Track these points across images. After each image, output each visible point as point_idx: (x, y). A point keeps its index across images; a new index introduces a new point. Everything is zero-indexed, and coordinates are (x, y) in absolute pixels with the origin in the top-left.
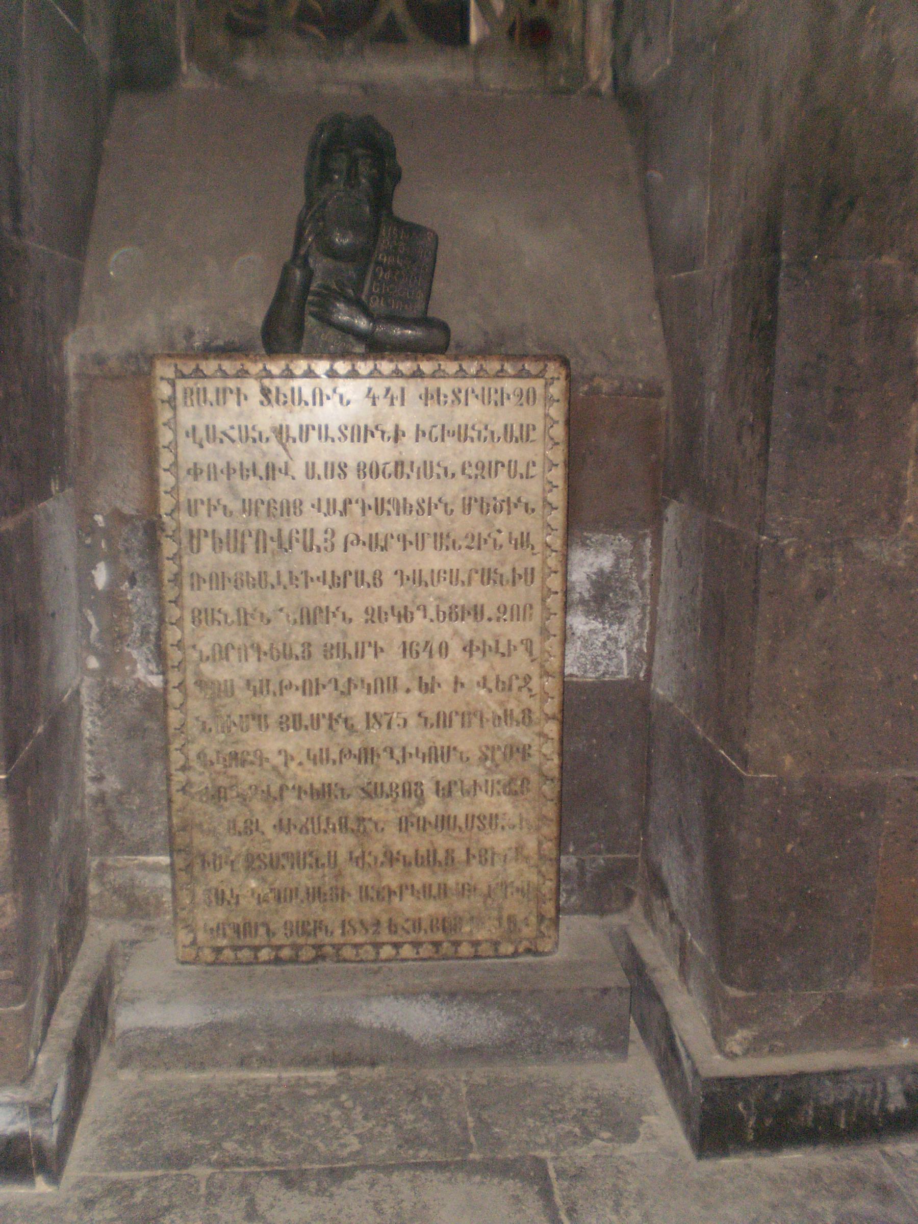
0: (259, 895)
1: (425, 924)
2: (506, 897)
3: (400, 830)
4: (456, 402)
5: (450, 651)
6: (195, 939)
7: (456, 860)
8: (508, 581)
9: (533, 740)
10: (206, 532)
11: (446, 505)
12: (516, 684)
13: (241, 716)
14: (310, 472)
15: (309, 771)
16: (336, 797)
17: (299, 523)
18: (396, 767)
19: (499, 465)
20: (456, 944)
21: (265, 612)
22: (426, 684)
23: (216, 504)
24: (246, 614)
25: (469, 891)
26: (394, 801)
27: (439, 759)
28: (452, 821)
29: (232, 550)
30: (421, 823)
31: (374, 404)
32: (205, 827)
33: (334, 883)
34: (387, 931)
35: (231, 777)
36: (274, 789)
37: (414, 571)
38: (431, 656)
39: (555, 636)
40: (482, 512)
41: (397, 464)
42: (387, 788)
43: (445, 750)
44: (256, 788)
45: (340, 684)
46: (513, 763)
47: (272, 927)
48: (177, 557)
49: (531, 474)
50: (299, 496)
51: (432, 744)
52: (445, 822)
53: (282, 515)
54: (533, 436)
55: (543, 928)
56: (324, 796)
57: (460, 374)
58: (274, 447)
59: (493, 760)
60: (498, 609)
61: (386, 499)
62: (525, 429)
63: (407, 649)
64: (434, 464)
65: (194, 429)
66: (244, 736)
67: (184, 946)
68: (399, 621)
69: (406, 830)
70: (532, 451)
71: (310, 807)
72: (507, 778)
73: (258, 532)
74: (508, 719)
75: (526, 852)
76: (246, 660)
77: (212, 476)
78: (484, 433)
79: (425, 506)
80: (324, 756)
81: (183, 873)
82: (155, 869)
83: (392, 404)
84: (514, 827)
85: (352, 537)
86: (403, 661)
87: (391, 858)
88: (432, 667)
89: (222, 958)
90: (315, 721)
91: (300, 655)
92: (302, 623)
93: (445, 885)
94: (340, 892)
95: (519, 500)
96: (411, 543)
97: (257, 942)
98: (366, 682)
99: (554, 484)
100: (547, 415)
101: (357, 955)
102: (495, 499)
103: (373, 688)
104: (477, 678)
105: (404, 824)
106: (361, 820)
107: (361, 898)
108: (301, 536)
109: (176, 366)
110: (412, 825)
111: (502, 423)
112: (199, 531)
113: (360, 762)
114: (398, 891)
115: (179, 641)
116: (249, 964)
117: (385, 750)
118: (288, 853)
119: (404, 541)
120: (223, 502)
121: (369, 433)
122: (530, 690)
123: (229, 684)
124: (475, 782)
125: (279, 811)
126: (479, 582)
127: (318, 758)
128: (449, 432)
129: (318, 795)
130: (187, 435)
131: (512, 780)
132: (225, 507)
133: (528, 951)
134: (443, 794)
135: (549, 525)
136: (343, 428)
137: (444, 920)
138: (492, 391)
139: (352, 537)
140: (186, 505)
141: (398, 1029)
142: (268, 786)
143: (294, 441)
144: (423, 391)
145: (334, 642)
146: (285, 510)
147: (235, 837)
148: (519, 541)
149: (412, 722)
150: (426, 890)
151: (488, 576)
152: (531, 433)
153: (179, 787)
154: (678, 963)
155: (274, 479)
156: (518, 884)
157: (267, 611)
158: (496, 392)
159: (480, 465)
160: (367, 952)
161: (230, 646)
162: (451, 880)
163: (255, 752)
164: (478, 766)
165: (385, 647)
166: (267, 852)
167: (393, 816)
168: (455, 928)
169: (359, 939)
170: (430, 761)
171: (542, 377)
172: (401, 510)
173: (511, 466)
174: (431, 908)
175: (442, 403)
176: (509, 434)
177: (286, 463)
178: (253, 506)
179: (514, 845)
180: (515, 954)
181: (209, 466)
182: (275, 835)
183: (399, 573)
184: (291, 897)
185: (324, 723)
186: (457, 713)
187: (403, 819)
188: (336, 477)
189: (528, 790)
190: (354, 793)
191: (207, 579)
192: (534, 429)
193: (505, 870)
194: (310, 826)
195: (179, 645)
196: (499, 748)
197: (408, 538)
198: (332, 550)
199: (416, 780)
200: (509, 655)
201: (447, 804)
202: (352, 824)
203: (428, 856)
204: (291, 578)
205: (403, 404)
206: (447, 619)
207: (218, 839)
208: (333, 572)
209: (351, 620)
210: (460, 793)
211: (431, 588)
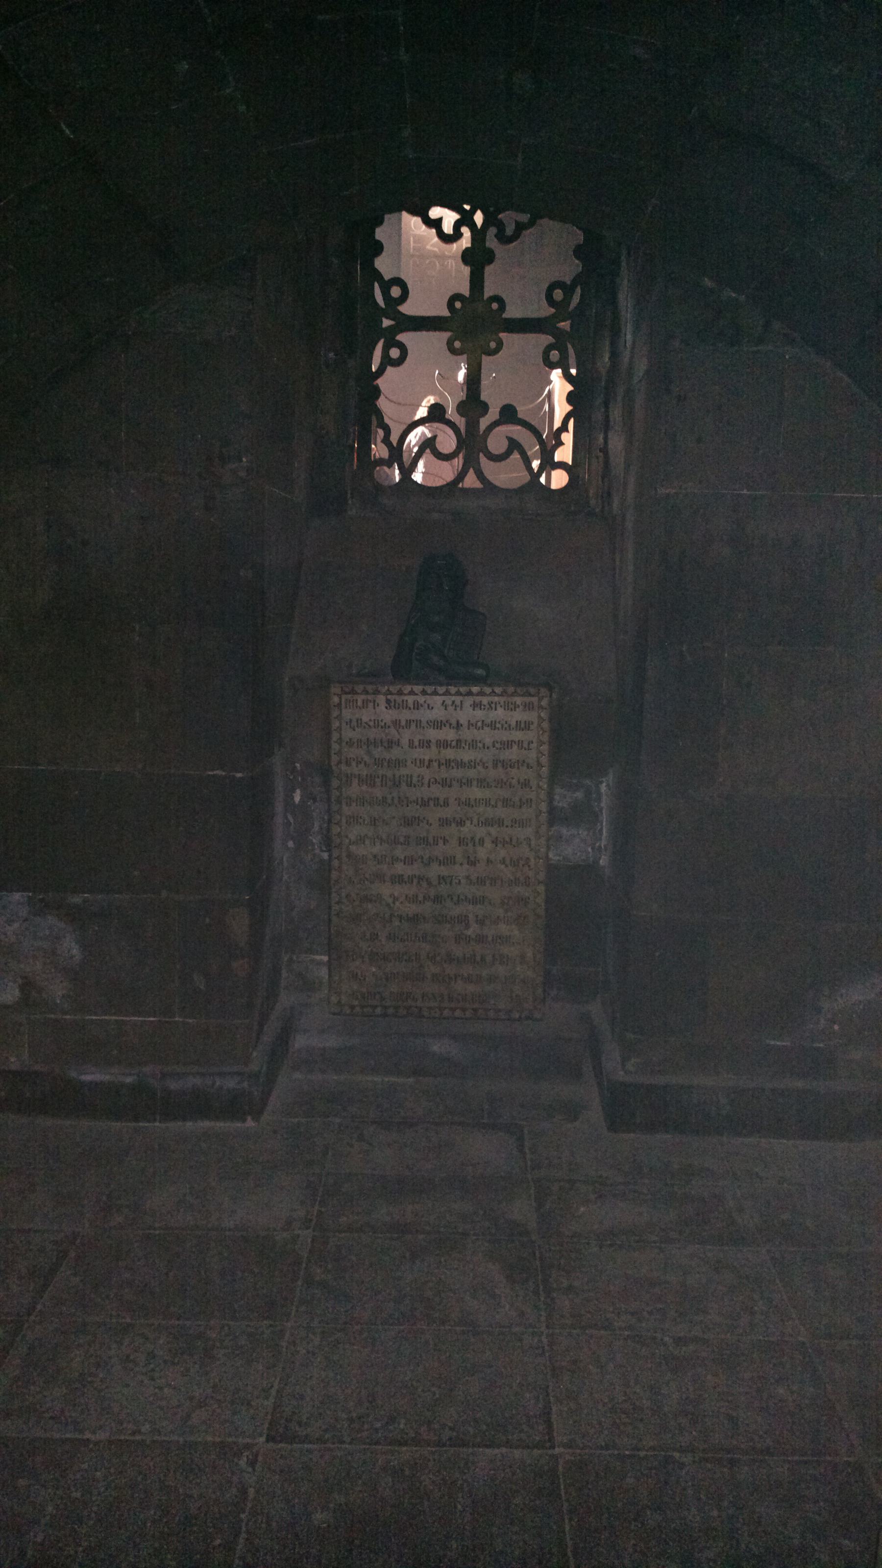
12: (522, 863)
17: (404, 771)
31: (446, 709)
38: (474, 845)
41: (457, 740)
45: (425, 861)
48: (339, 788)
52: (481, 939)
54: (532, 727)
58: (393, 731)
63: (461, 841)
64: (478, 741)
79: (473, 764)
82: (319, 963)
83: (456, 710)
86: (459, 848)
87: (450, 958)
88: (475, 852)
89: (354, 1011)
90: (411, 879)
102: (510, 760)
108: (405, 778)
109: (342, 688)
114: (454, 977)
117: (448, 896)
122: (529, 866)
132: (365, 762)
144: (472, 703)
151: (506, 802)
152: (531, 726)
169: (433, 1004)
173: (520, 743)
174: (471, 988)
185: (415, 881)
208: (422, 799)
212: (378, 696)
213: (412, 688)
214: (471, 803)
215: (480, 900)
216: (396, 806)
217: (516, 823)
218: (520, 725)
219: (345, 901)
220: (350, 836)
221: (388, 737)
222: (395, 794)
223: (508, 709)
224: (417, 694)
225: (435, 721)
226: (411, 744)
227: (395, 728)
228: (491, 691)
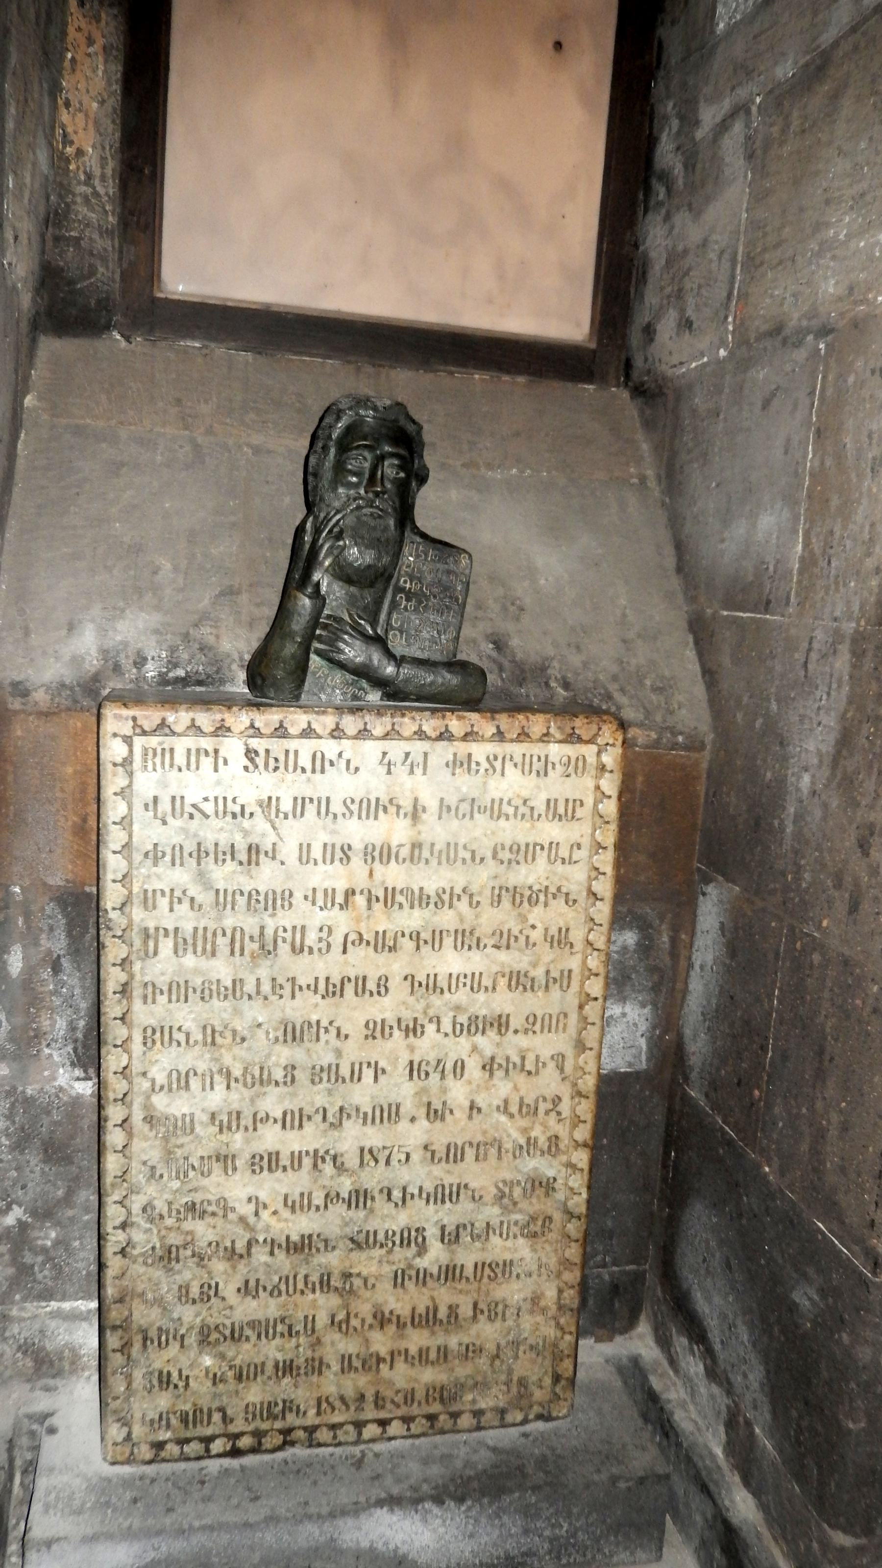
0: (215, 1375)
1: (420, 1395)
2: (516, 1357)
3: (395, 1285)
4: (491, 771)
5: (466, 1070)
6: (129, 1434)
7: (460, 1317)
8: (540, 988)
9: (559, 1171)
10: (166, 930)
11: (471, 896)
13: (202, 1158)
14: (305, 854)
15: (286, 1220)
16: (318, 1250)
17: (286, 919)
18: (394, 1211)
19: (538, 848)
20: (455, 1416)
21: (239, 1028)
22: (436, 1111)
23: (181, 895)
25: (474, 1352)
26: (390, 1252)
27: (447, 1199)
28: (458, 1271)
29: (199, 954)
30: (421, 1275)
31: (389, 772)
32: (150, 1296)
33: (309, 1353)
34: (372, 1406)
35: (187, 1233)
36: (240, 1246)
38: (443, 1077)
39: (591, 1049)
40: (514, 904)
42: (381, 1237)
43: (455, 1189)
44: (218, 1244)
46: (534, 1200)
47: (229, 1412)
49: (575, 858)
50: (289, 885)
51: (439, 1182)
53: (266, 909)
54: (579, 813)
55: (558, 1390)
58: (260, 825)
59: (511, 1195)
60: (527, 1019)
61: (399, 888)
64: (460, 848)
65: (156, 799)
66: (205, 1182)
67: (115, 1444)
68: (407, 1036)
70: (580, 831)
71: (283, 1261)
72: (527, 1218)
73: (235, 929)
75: (543, 1303)
76: (212, 1088)
77: (178, 861)
79: (446, 897)
81: (119, 1354)
82: (75, 1317)
83: (412, 772)
85: (353, 937)
87: (382, 1320)
88: (444, 1090)
89: (163, 1454)
90: (297, 1160)
91: (280, 1079)
92: (285, 1041)
93: (446, 1347)
94: (317, 1364)
95: (559, 889)
96: (426, 942)
97: (209, 1431)
98: (362, 1111)
99: (601, 870)
100: (598, 788)
101: (335, 1437)
102: (530, 888)
104: (496, 1102)
105: (399, 1280)
106: (347, 1276)
107: (343, 1371)
108: (288, 935)
109: (134, 719)
110: (410, 1278)
111: (543, 797)
112: (157, 929)
113: (349, 1206)
114: (388, 1359)
115: (125, 1068)
116: (199, 1458)
117: (381, 1191)
118: (254, 1321)
119: (418, 938)
120: (190, 893)
121: (381, 808)
122: (559, 1113)
123: (188, 1119)
124: (488, 1224)
125: (245, 1271)
126: (505, 987)
127: (298, 1205)
129: (295, 1249)
130: (146, 806)
131: (533, 1219)
132: (192, 899)
133: (540, 1417)
134: (450, 1240)
135: (592, 920)
136: (349, 801)
137: (442, 1388)
138: (535, 759)
139: (353, 937)
140: (142, 896)
141: (391, 1546)
142: (233, 1242)
143: (286, 817)
144: (451, 758)
145: (325, 1063)
146: (270, 902)
147: (187, 1306)
148: (556, 938)
149: (415, 1157)
150: (423, 1356)
153: (117, 1249)
154: (723, 1436)
155: (257, 864)
156: (532, 1341)
157: (240, 1026)
159: (515, 847)
160: (346, 1433)
162: (453, 1342)
163: (218, 1201)
164: (493, 1204)
165: (388, 1069)
166: (228, 1323)
167: (388, 1270)
168: (454, 1398)
169: (337, 1418)
170: (435, 1202)
171: (593, 743)
172: (416, 902)
174: (428, 1375)
175: (473, 772)
176: (552, 810)
177: (274, 844)
178: (229, 898)
179: (529, 1296)
180: (525, 1421)
181: (174, 848)
182: (240, 1299)
183: (409, 978)
184: (256, 1375)
186: (471, 1144)
187: (400, 1272)
189: (550, 1230)
190: (341, 1245)
191: (165, 988)
192: (582, 805)
193: (518, 1326)
194: (283, 1287)
195: (124, 1072)
196: (519, 1183)
197: (423, 936)
198: (328, 951)
199: (418, 1225)
200: (537, 1073)
201: (453, 1252)
202: (336, 1282)
203: (427, 1314)
204: (273, 987)
205: (424, 774)
206: (465, 1032)
207: (165, 1309)
208: (328, 979)
209: (347, 1037)
210: (469, 1238)
211: (447, 995)
213: (309, 723)
214: (438, 984)
216: (266, 998)
217: (534, 1024)
218: (555, 809)
219: (139, 1219)
221: (249, 840)
222: (264, 972)
223: (531, 772)
224: (320, 737)
225: (361, 801)
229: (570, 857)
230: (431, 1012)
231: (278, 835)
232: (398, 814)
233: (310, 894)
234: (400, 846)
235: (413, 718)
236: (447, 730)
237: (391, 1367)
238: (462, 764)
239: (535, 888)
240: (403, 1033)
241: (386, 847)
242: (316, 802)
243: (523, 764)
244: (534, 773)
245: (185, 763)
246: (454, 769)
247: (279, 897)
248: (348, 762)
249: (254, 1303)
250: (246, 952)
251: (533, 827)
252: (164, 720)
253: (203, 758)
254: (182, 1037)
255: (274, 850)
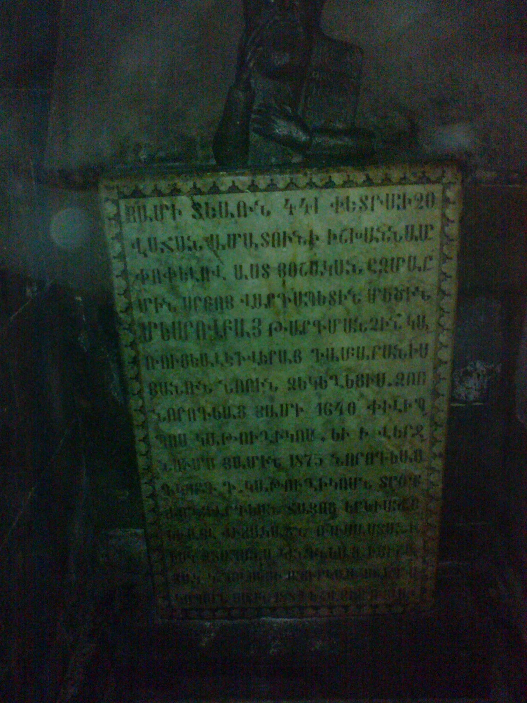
4: (364, 208)
8: (405, 355)
10: (155, 324)
11: (354, 296)
12: (410, 433)
13: (193, 460)
17: (230, 315)
19: (401, 261)
21: (207, 384)
22: (338, 434)
24: (192, 386)
26: (314, 516)
27: (348, 487)
31: (291, 213)
35: (190, 501)
36: (221, 508)
37: (328, 349)
38: (341, 413)
42: (307, 508)
43: (353, 480)
45: (269, 436)
48: (133, 345)
51: (343, 476)
54: (430, 234)
56: (260, 511)
57: (367, 183)
58: (208, 253)
59: (391, 486)
60: (397, 376)
61: (304, 292)
62: (424, 229)
63: (321, 409)
64: (344, 262)
66: (196, 473)
68: (316, 388)
69: (323, 535)
74: (403, 457)
76: (195, 420)
77: (157, 280)
78: (388, 234)
79: (337, 297)
80: (259, 485)
83: (307, 211)
84: (405, 532)
87: (311, 553)
88: (343, 421)
90: (251, 462)
91: (237, 415)
92: (237, 392)
95: (417, 289)
96: (325, 328)
100: (443, 215)
102: (396, 289)
103: (295, 437)
104: (378, 429)
106: (288, 529)
108: (233, 325)
109: (118, 187)
111: (403, 225)
112: (150, 323)
113: (286, 490)
117: (305, 481)
121: (287, 239)
122: (421, 436)
123: (182, 437)
124: (376, 502)
127: (254, 487)
128: (357, 234)
134: (351, 511)
136: (265, 235)
137: (351, 591)
139: (275, 325)
142: (217, 507)
144: (334, 200)
146: (219, 305)
149: (326, 462)
155: (208, 280)
158: (399, 197)
159: (384, 261)
161: (181, 410)
163: (206, 484)
165: (305, 408)
170: (341, 488)
171: (439, 183)
172: (316, 302)
174: (342, 585)
175: (351, 209)
177: (218, 267)
178: (193, 303)
188: (260, 276)
191: (159, 360)
192: (432, 228)
194: (250, 533)
195: (142, 410)
196: (396, 478)
197: (322, 323)
205: (316, 212)
206: (354, 385)
208: (261, 353)
209: (276, 388)
211: (341, 362)
212: (179, 198)
215: (350, 483)
216: (222, 365)
217: (402, 379)
218: (412, 232)
220: (158, 409)
221: (201, 264)
223: (393, 207)
224: (241, 191)
225: (273, 235)
226: (238, 270)
227: (212, 249)
228: (364, 178)
229: (425, 266)
230: (331, 373)
231: (220, 260)
232: (299, 242)
233: (244, 298)
234: (303, 264)
235: (306, 174)
236: (330, 180)
237: (319, 579)
238: (342, 204)
239: (399, 289)
240: (313, 386)
241: (293, 266)
242: (243, 237)
243: (387, 202)
244: (396, 207)
245: (154, 215)
246: (337, 208)
247: (224, 301)
248: (262, 208)
249: (233, 541)
250: (207, 337)
251: (396, 246)
252: (137, 187)
253: (165, 211)
254: (173, 389)
255: (218, 270)
